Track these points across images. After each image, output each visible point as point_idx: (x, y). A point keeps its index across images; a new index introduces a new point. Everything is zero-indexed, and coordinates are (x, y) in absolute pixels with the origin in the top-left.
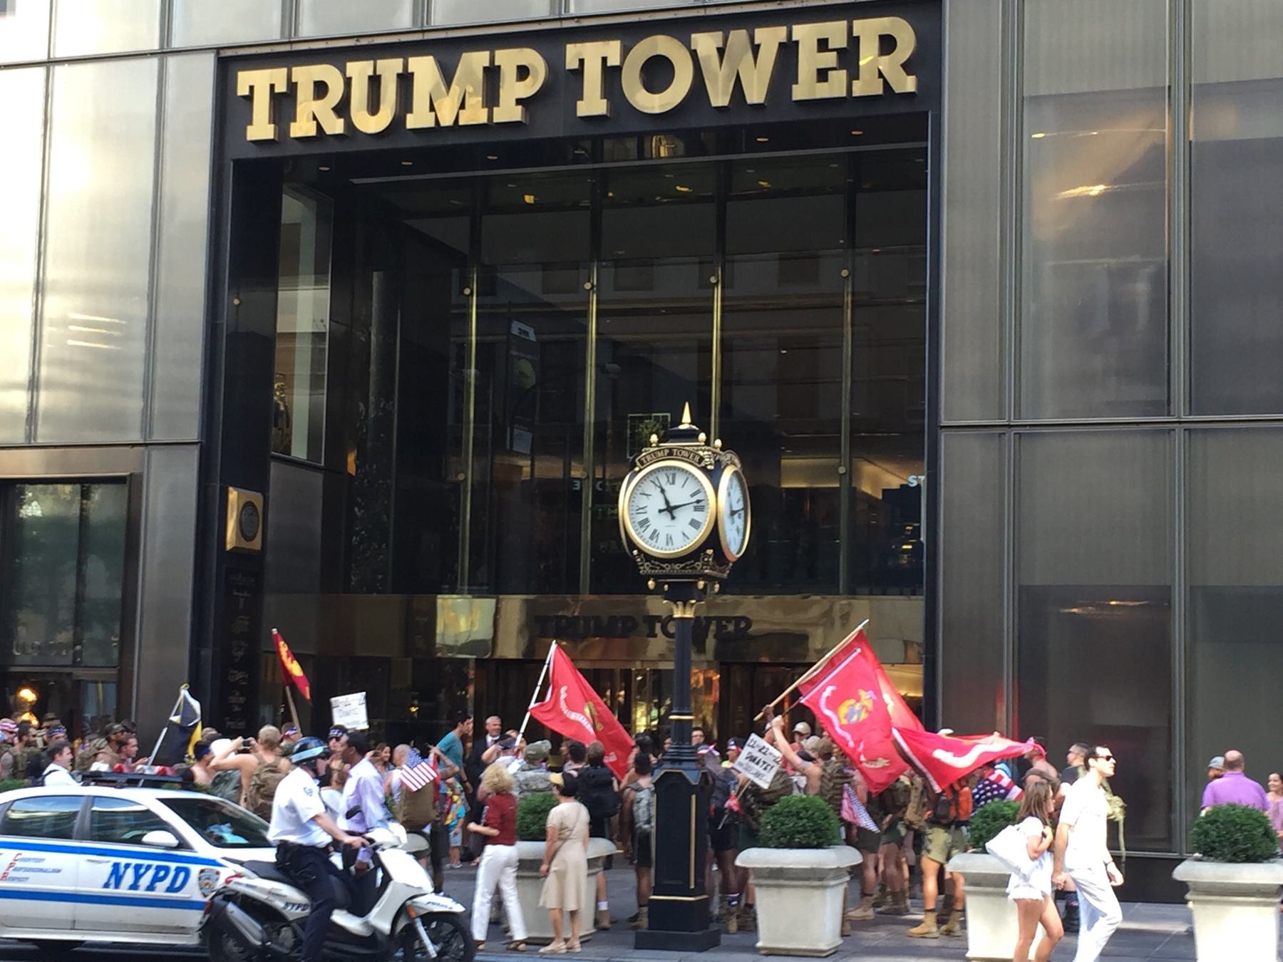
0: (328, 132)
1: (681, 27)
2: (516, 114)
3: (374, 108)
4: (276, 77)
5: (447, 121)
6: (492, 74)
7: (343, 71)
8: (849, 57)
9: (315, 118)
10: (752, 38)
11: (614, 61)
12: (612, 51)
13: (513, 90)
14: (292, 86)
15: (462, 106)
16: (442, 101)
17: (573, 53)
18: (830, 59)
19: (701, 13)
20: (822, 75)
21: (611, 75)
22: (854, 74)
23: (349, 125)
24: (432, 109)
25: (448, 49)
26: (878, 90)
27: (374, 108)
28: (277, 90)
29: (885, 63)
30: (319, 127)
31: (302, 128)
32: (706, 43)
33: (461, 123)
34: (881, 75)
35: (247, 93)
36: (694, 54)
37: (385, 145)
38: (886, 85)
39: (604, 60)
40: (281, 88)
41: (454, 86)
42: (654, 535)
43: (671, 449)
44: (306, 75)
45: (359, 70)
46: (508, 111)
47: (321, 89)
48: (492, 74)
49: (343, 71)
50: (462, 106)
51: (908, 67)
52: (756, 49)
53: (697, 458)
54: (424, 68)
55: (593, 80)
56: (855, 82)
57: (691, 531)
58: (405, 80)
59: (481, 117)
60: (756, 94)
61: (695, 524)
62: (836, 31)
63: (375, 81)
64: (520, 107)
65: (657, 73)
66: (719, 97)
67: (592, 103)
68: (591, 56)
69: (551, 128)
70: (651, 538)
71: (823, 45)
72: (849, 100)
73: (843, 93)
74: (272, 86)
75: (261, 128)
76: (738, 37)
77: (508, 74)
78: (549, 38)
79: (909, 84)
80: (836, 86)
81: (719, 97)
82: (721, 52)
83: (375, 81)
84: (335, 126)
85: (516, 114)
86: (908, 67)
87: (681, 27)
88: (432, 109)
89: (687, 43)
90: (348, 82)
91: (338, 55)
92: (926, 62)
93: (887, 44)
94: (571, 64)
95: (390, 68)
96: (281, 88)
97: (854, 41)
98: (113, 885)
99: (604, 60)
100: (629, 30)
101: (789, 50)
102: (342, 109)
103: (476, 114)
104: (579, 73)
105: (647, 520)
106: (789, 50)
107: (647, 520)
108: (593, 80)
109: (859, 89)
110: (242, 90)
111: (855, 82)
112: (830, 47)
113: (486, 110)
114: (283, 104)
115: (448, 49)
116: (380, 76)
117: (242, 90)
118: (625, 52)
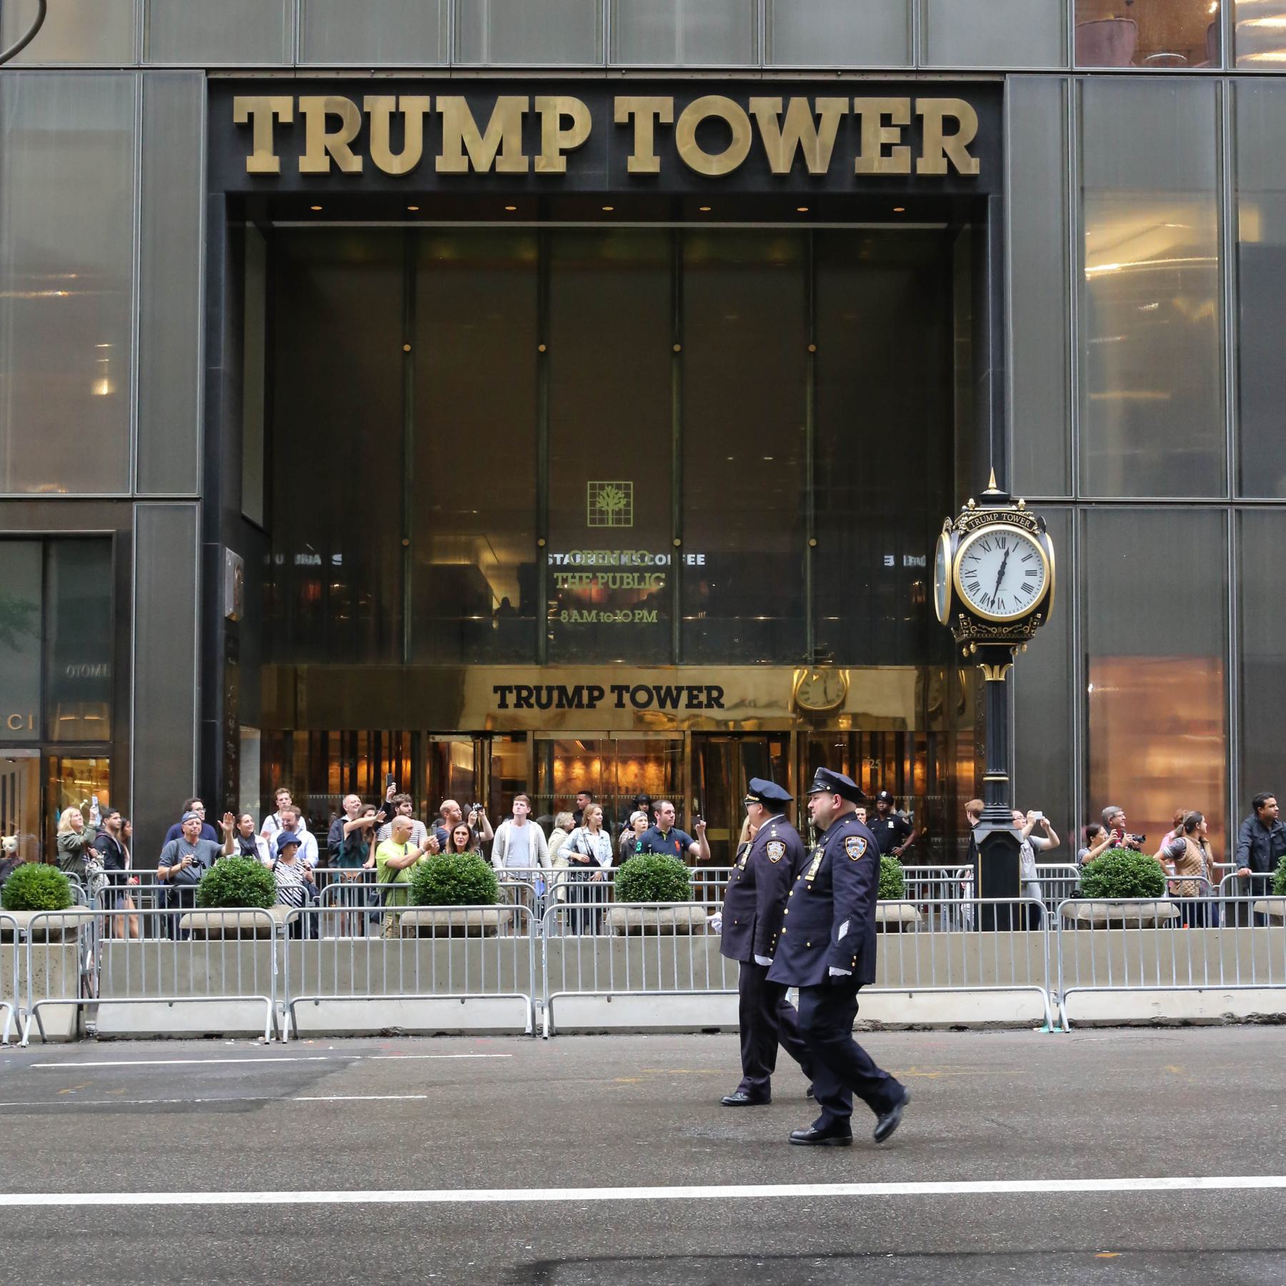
0: (344, 169)
1: (741, 89)
2: (560, 165)
3: (397, 145)
4: (283, 106)
5: (482, 166)
6: (531, 122)
7: (361, 107)
8: (913, 133)
9: (327, 153)
10: (812, 106)
11: (666, 118)
12: (664, 105)
13: (555, 141)
14: (300, 118)
16: (479, 143)
17: (624, 106)
19: (758, 77)
20: (886, 150)
21: (664, 133)
22: (917, 152)
23: (368, 162)
24: (465, 151)
25: (481, 91)
26: (942, 169)
27: (397, 145)
29: (951, 143)
30: (333, 163)
31: (314, 162)
32: (765, 106)
33: (498, 170)
34: (945, 155)
35: (245, 120)
36: (753, 118)
37: (407, 188)
38: (951, 165)
39: (656, 116)
40: (287, 117)
43: (1000, 514)
44: (315, 107)
45: (381, 106)
46: (549, 162)
47: (333, 123)
48: (531, 122)
49: (361, 107)
50: (499, 152)
51: (971, 148)
52: (817, 119)
53: (1028, 523)
54: (453, 108)
55: (644, 134)
56: (919, 160)
57: (1023, 596)
58: (433, 121)
60: (818, 165)
61: (1027, 588)
62: (898, 107)
63: (397, 119)
64: (564, 158)
65: (714, 133)
66: (781, 163)
67: (644, 160)
68: (641, 110)
69: (597, 178)
71: (886, 120)
72: (914, 178)
73: (905, 169)
75: (263, 160)
76: (799, 104)
77: (550, 124)
78: (597, 90)
79: (971, 166)
80: (899, 164)
81: (781, 163)
82: (781, 118)
83: (397, 119)
84: (354, 164)
85: (560, 165)
86: (971, 148)
87: (740, 89)
89: (746, 108)
90: (366, 117)
91: (358, 87)
92: (989, 145)
93: (950, 125)
94: (621, 117)
95: (415, 106)
97: (918, 120)
99: (656, 116)
100: (683, 88)
101: (850, 125)
102: (360, 145)
103: (513, 163)
104: (627, 129)
105: (977, 584)
106: (850, 125)
107: (977, 584)
108: (644, 134)
109: (924, 167)
110: (240, 117)
111: (919, 160)
112: (893, 122)
113: (526, 158)
114: (289, 136)
115: (481, 91)
116: (403, 114)
118: (677, 112)
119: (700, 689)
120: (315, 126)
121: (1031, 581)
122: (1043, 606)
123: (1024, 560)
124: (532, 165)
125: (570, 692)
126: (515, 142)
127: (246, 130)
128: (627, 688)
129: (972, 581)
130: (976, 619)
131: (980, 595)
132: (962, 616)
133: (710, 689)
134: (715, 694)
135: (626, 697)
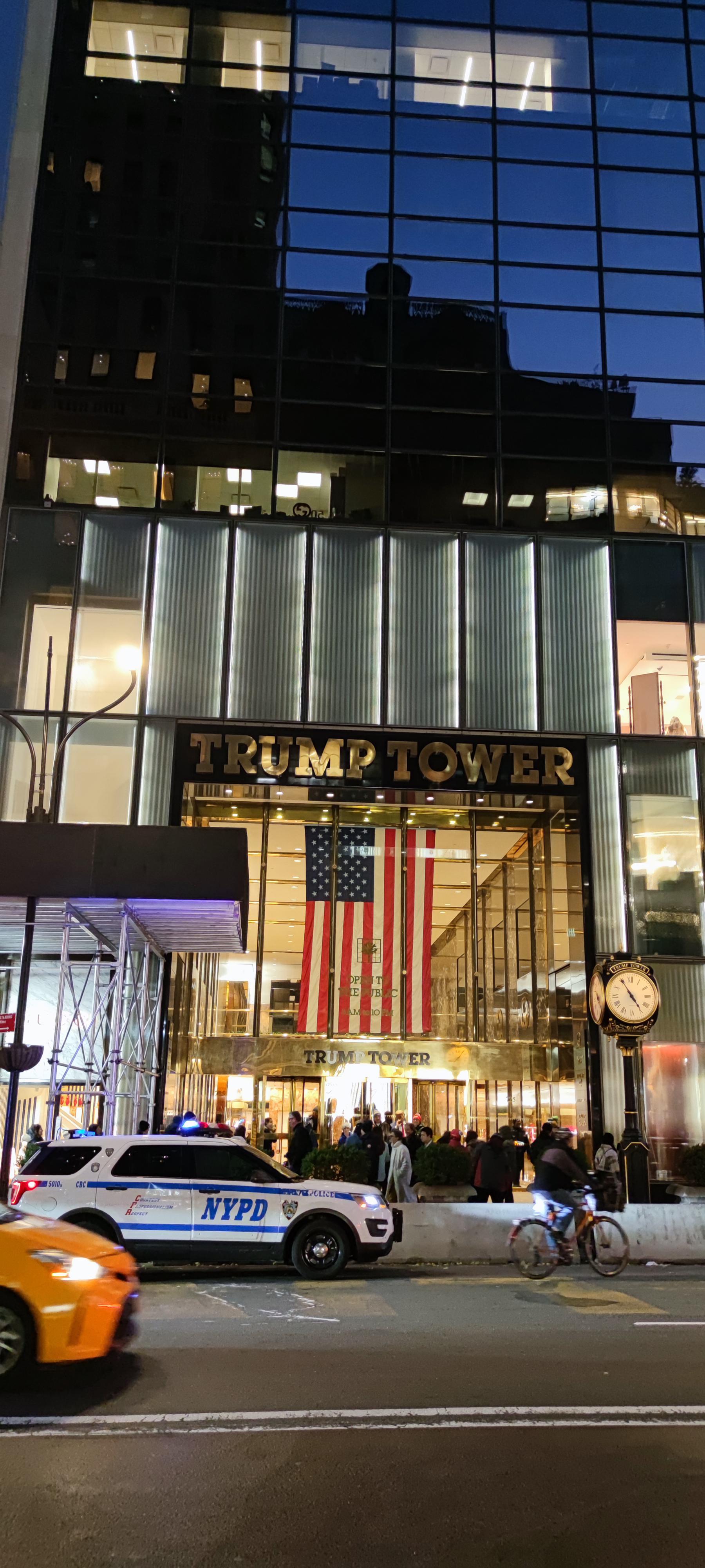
4: (216, 738)
14: (225, 746)
15: (328, 766)
18: (529, 764)
24: (310, 765)
28: (216, 746)
40: (218, 745)
41: (324, 755)
42: (623, 1010)
50: (328, 766)
59: (339, 773)
61: (645, 1005)
70: (622, 1011)
74: (213, 744)
88: (310, 765)
89: (455, 749)
96: (218, 745)
98: (209, 1216)
103: (336, 771)
110: (193, 744)
117: (193, 744)
119: (417, 1054)
120: (233, 750)
121: (648, 1001)
122: (655, 1016)
123: (644, 989)
124: (345, 773)
125: (346, 1054)
126: (336, 760)
127: (198, 750)
128: (377, 1053)
129: (616, 1000)
130: (618, 1021)
131: (621, 1008)
132: (611, 1019)
133: (422, 1055)
134: (425, 1057)
135: (377, 1058)
